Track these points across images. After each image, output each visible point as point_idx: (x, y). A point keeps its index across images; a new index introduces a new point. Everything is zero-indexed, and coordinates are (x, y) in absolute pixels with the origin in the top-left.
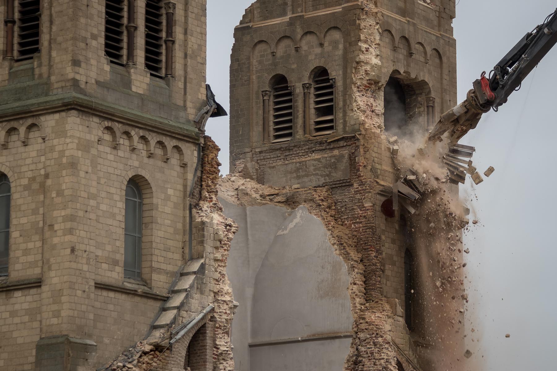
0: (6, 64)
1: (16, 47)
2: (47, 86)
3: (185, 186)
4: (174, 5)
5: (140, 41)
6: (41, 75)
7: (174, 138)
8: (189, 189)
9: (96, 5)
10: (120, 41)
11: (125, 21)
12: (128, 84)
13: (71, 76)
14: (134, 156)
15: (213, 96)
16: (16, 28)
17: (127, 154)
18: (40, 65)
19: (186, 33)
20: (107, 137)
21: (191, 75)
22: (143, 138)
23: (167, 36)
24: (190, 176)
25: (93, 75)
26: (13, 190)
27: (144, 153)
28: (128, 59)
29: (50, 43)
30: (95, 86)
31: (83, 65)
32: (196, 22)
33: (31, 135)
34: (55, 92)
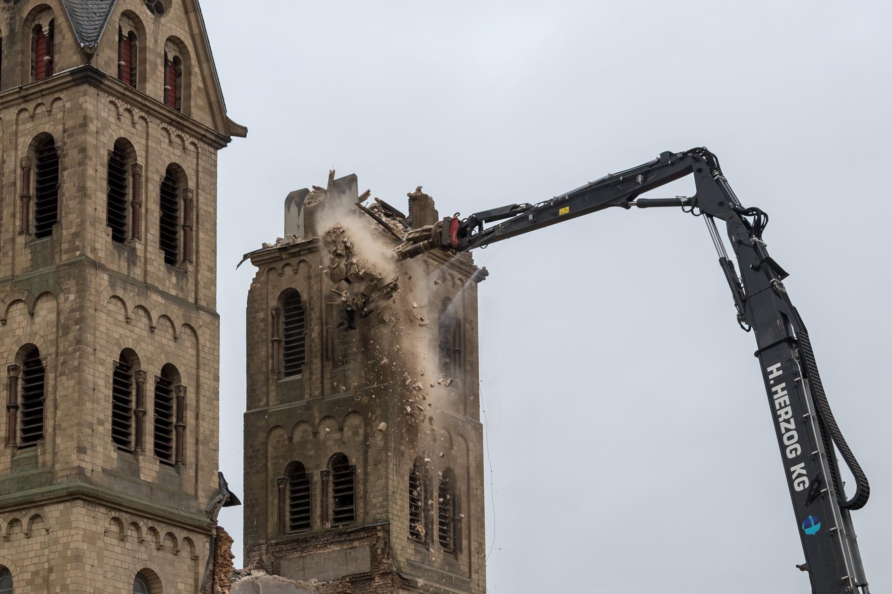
0: (9, 451)
1: (19, 434)
2: (50, 475)
3: (196, 580)
4: (185, 388)
5: (149, 426)
6: (44, 463)
7: (185, 529)
8: (200, 583)
9: (103, 389)
10: (127, 427)
11: (133, 405)
12: (136, 472)
13: (76, 464)
14: (143, 549)
15: (226, 484)
16: (19, 414)
17: (136, 547)
18: (44, 453)
19: (197, 418)
20: (114, 528)
21: (203, 462)
22: (152, 529)
23: (178, 421)
24: (202, 570)
25: (100, 462)
26: (15, 585)
27: (153, 545)
28: (136, 445)
29: (54, 430)
30: (102, 475)
31: (89, 452)
32: (208, 407)
33: (35, 527)
34: (59, 480)
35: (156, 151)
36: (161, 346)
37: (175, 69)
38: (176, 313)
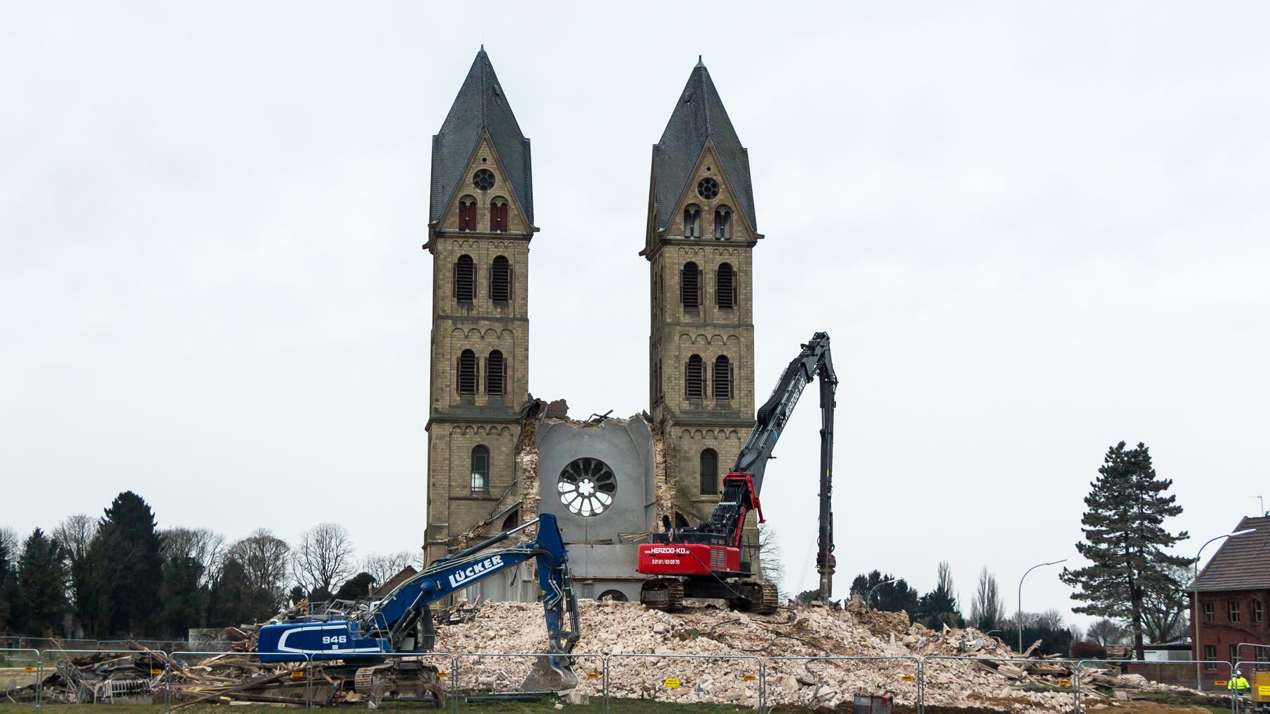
5: (482, 381)
12: (472, 403)
24: (515, 440)
25: (447, 403)
35: (483, 255)
36: (490, 344)
37: (499, 212)
38: (498, 327)
